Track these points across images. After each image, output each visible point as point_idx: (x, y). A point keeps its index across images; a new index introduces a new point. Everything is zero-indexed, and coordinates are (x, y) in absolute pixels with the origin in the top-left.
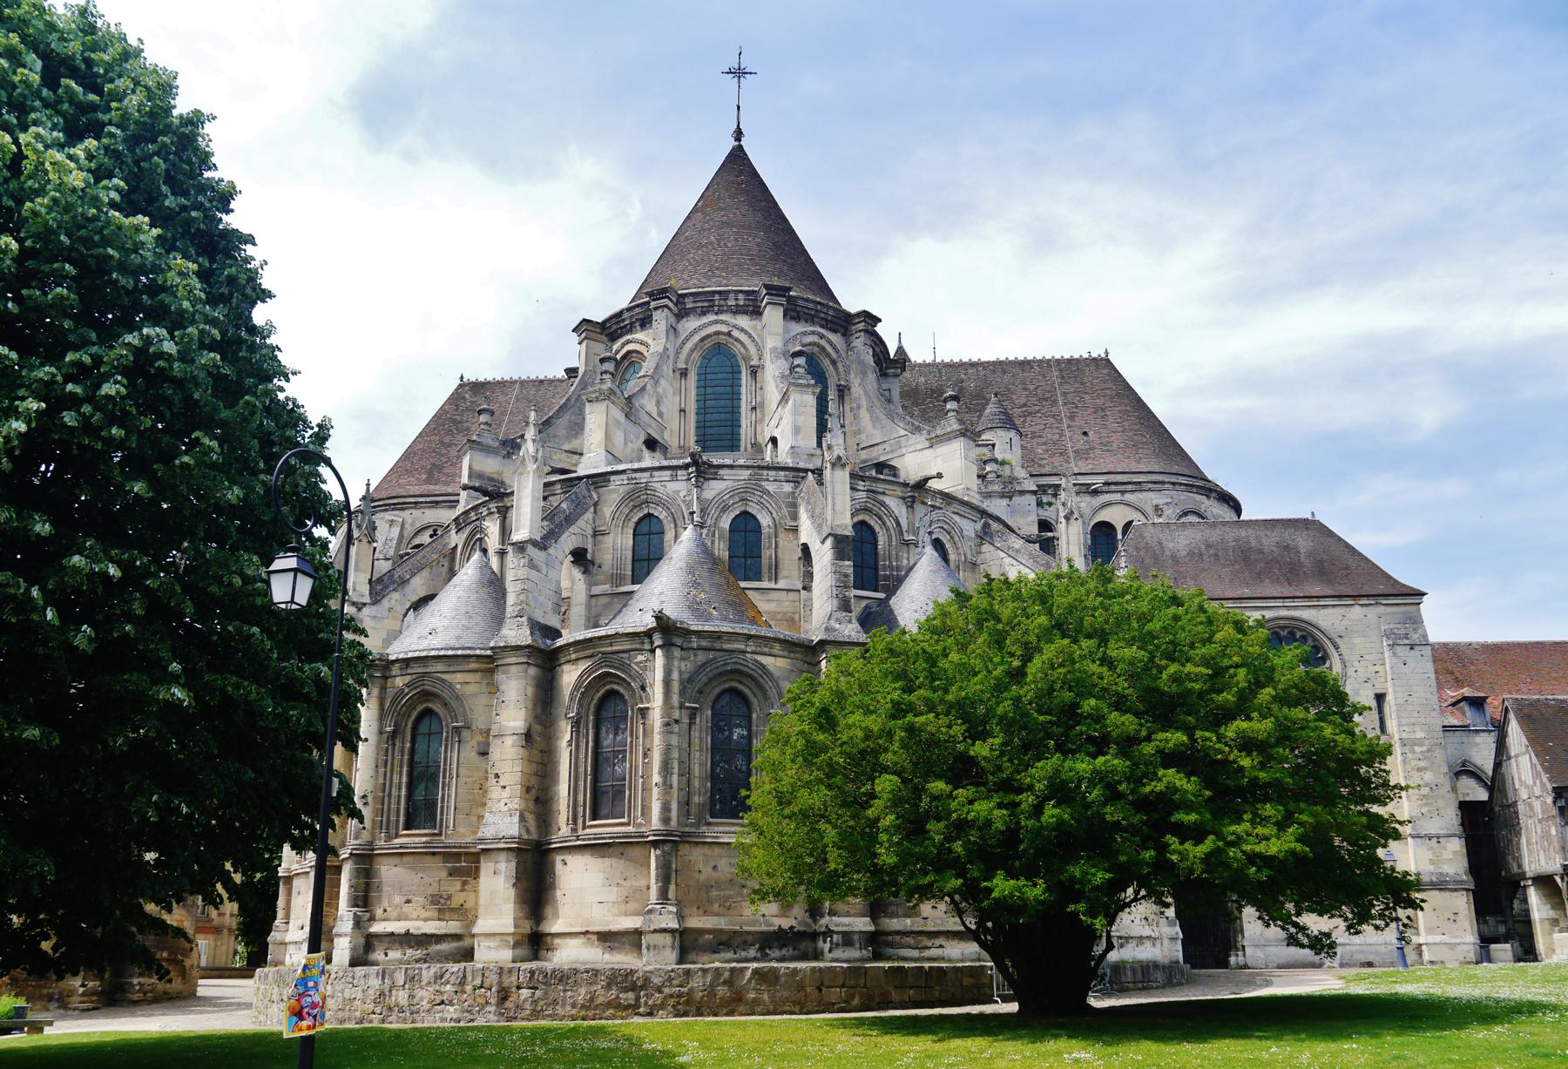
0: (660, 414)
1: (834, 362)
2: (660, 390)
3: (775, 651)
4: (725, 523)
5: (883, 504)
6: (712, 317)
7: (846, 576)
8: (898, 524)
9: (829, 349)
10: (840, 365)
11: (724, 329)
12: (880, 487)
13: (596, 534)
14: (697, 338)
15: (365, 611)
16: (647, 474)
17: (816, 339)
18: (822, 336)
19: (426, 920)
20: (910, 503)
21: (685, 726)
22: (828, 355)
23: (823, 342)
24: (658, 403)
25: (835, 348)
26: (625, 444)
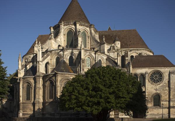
0: (61, 41)
1: (87, 32)
2: (61, 37)
4: (68, 58)
5: (91, 54)
6: (69, 26)
7: (83, 65)
9: (86, 30)
10: (88, 33)
11: (70, 28)
12: (91, 52)
13: (50, 59)
14: (66, 29)
15: (21, 71)
17: (84, 29)
18: (85, 28)
20: (95, 54)
22: (86, 32)
23: (86, 29)
24: (61, 40)
25: (87, 30)
26: (55, 46)
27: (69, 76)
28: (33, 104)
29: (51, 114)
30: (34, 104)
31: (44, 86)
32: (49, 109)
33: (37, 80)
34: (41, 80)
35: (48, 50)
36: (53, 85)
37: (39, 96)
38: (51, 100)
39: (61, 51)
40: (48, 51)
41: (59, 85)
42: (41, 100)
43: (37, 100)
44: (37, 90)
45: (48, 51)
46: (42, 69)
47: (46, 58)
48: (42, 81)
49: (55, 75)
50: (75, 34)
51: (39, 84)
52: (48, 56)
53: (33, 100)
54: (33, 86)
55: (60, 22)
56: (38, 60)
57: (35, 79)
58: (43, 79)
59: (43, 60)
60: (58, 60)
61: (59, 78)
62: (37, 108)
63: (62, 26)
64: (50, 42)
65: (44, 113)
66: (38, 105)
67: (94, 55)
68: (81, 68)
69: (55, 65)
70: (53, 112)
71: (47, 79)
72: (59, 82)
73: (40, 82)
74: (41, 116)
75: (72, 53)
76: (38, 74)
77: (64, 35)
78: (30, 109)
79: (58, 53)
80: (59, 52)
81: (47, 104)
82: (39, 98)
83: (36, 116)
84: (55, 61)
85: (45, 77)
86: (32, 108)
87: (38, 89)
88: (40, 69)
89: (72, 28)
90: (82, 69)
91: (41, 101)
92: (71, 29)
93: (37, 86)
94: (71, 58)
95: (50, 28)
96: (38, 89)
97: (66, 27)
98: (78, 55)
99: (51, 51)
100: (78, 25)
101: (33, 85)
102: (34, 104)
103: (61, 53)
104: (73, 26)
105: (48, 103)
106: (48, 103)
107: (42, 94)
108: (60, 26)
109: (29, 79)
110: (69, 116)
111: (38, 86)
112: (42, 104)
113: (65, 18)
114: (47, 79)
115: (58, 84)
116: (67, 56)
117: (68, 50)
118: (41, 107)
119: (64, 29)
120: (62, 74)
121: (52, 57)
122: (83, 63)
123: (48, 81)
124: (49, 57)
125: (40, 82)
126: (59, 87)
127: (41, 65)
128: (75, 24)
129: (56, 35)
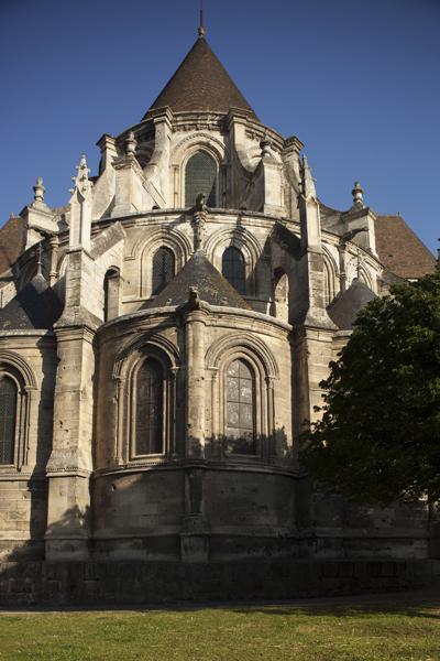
3: (270, 332)
4: (220, 253)
6: (194, 132)
7: (320, 282)
8: (335, 263)
11: (204, 140)
13: (126, 259)
14: (185, 145)
16: (163, 217)
19: (7, 530)
20: (341, 248)
21: (209, 384)
27: (256, 326)
28: (30, 483)
29: (150, 543)
30: (39, 488)
31: (104, 380)
32: (140, 512)
33: (67, 348)
34: (87, 348)
35: (113, 216)
36: (166, 377)
37: (75, 437)
38: (154, 459)
39: (182, 221)
40: (114, 220)
41: (203, 373)
42: (86, 464)
43: (58, 459)
44: (63, 405)
45: (114, 220)
46: (88, 300)
47: (109, 245)
48: (89, 358)
49: (180, 320)
50: (224, 169)
51: (79, 368)
52: (116, 238)
53: (32, 462)
54: (34, 383)
55: (158, 108)
56: (73, 245)
57: (50, 348)
58: (96, 345)
59: (99, 250)
60: (164, 261)
61: (203, 334)
62: (57, 507)
63: (164, 130)
64: (123, 180)
65: (105, 533)
66: (66, 489)
67: (335, 254)
68: (311, 293)
69: (149, 287)
70: (168, 531)
71: (128, 341)
72: (202, 353)
73: (84, 359)
74: (81, 554)
75: (238, 232)
76: (69, 316)
77: (176, 168)
78: (14, 515)
79: (169, 229)
80: (174, 224)
81: (123, 484)
82: (74, 450)
83: (51, 556)
84: (148, 266)
85: (109, 336)
86: (26, 507)
87: (69, 396)
88: (83, 292)
89: (212, 143)
90: (312, 300)
91: (84, 464)
92: (208, 145)
93: (66, 379)
94: (232, 254)
95: (102, 143)
96: (69, 396)
97: (182, 135)
98: (267, 244)
99: (128, 220)
100: (240, 131)
101: (39, 377)
102: (39, 488)
103: (186, 228)
104: (217, 135)
105: (134, 478)
106: (134, 478)
107: (89, 428)
108: (158, 127)
109: (13, 344)
110: (261, 553)
111: (71, 384)
112: (86, 483)
113: (175, 97)
114: (128, 341)
115: (199, 365)
116: (212, 245)
117: (218, 217)
118: (84, 502)
119: (175, 145)
120: (219, 314)
121: (134, 247)
122: (317, 268)
123: (135, 353)
124: (119, 248)
125: (80, 359)
126: (203, 383)
127: (86, 271)
128: (226, 127)
129: (146, 159)
